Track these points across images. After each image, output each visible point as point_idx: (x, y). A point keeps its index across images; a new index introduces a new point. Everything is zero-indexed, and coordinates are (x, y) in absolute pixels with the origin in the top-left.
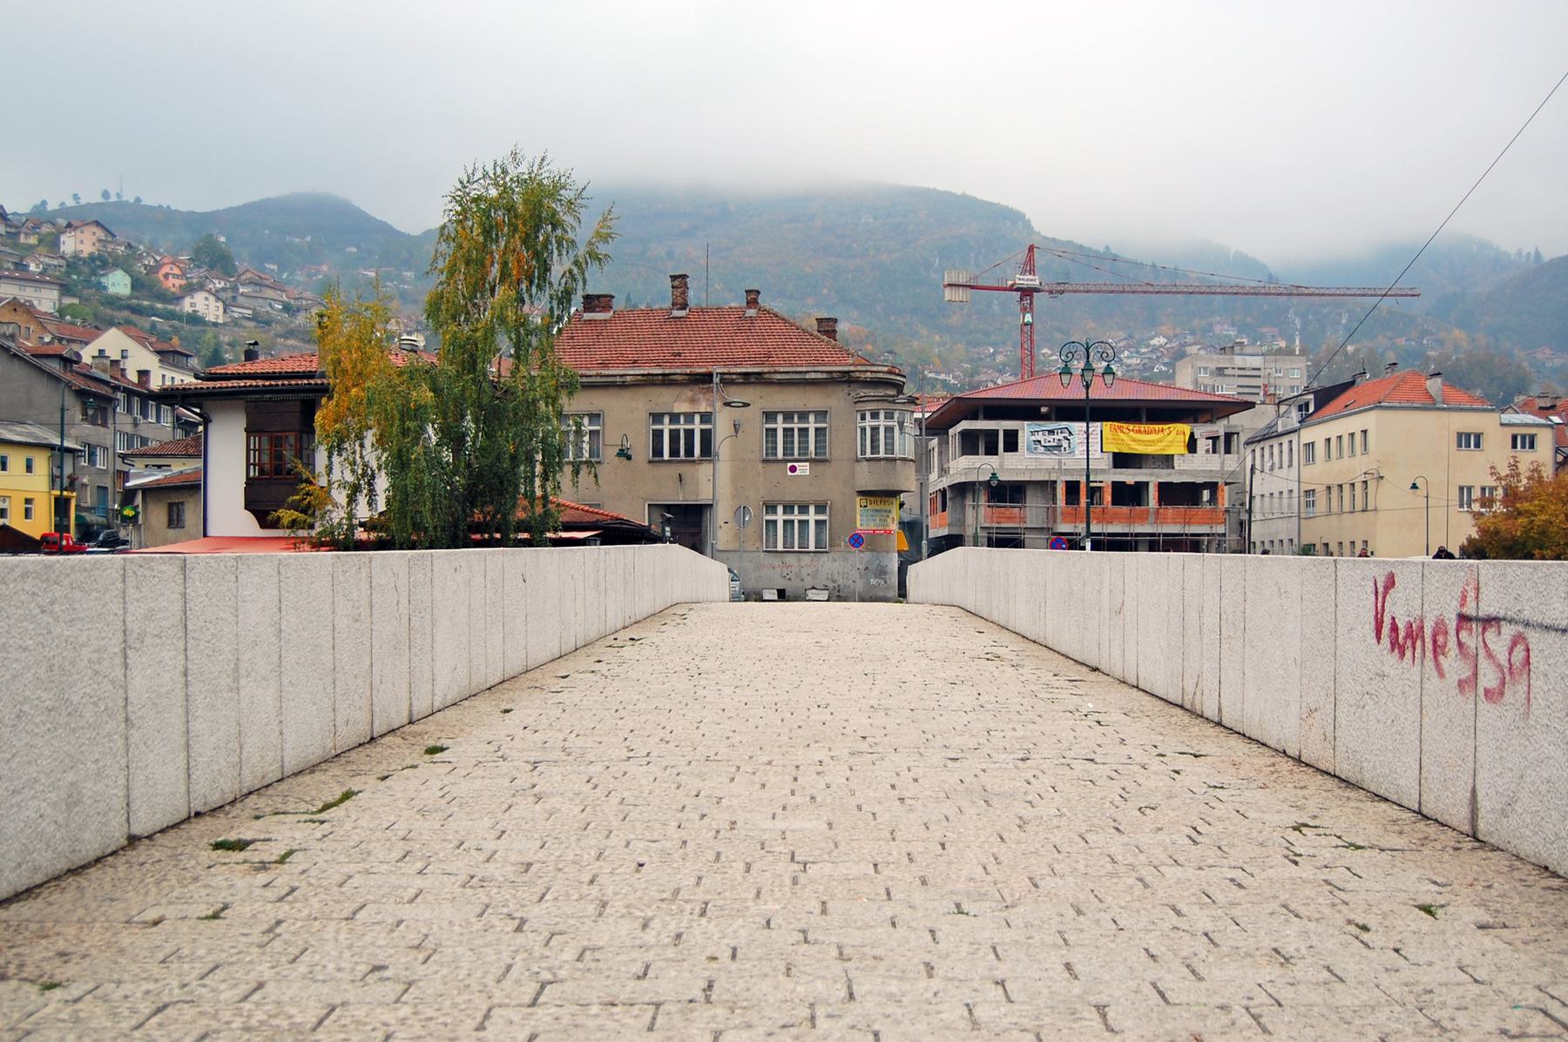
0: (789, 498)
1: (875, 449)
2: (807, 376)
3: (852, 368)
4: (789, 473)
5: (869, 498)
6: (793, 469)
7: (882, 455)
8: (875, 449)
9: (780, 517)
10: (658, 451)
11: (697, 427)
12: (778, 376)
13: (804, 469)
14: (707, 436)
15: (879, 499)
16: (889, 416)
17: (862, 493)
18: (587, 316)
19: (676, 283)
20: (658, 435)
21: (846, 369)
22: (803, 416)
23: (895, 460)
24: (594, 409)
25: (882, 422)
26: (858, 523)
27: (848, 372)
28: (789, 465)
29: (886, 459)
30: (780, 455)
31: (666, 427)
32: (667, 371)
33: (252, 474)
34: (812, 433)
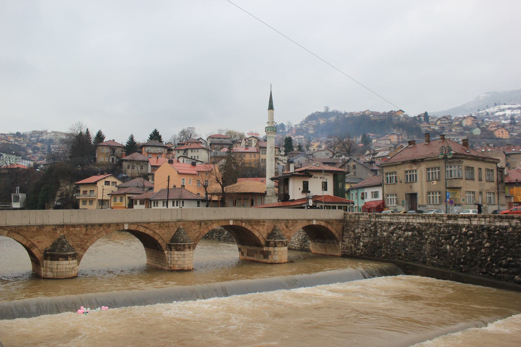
0: (433, 190)
6: (433, 183)
7: (449, 178)
12: (429, 159)
14: (416, 175)
19: (426, 136)
20: (407, 176)
22: (435, 168)
24: (395, 171)
28: (432, 182)
29: (450, 179)
30: (431, 179)
34: (437, 173)
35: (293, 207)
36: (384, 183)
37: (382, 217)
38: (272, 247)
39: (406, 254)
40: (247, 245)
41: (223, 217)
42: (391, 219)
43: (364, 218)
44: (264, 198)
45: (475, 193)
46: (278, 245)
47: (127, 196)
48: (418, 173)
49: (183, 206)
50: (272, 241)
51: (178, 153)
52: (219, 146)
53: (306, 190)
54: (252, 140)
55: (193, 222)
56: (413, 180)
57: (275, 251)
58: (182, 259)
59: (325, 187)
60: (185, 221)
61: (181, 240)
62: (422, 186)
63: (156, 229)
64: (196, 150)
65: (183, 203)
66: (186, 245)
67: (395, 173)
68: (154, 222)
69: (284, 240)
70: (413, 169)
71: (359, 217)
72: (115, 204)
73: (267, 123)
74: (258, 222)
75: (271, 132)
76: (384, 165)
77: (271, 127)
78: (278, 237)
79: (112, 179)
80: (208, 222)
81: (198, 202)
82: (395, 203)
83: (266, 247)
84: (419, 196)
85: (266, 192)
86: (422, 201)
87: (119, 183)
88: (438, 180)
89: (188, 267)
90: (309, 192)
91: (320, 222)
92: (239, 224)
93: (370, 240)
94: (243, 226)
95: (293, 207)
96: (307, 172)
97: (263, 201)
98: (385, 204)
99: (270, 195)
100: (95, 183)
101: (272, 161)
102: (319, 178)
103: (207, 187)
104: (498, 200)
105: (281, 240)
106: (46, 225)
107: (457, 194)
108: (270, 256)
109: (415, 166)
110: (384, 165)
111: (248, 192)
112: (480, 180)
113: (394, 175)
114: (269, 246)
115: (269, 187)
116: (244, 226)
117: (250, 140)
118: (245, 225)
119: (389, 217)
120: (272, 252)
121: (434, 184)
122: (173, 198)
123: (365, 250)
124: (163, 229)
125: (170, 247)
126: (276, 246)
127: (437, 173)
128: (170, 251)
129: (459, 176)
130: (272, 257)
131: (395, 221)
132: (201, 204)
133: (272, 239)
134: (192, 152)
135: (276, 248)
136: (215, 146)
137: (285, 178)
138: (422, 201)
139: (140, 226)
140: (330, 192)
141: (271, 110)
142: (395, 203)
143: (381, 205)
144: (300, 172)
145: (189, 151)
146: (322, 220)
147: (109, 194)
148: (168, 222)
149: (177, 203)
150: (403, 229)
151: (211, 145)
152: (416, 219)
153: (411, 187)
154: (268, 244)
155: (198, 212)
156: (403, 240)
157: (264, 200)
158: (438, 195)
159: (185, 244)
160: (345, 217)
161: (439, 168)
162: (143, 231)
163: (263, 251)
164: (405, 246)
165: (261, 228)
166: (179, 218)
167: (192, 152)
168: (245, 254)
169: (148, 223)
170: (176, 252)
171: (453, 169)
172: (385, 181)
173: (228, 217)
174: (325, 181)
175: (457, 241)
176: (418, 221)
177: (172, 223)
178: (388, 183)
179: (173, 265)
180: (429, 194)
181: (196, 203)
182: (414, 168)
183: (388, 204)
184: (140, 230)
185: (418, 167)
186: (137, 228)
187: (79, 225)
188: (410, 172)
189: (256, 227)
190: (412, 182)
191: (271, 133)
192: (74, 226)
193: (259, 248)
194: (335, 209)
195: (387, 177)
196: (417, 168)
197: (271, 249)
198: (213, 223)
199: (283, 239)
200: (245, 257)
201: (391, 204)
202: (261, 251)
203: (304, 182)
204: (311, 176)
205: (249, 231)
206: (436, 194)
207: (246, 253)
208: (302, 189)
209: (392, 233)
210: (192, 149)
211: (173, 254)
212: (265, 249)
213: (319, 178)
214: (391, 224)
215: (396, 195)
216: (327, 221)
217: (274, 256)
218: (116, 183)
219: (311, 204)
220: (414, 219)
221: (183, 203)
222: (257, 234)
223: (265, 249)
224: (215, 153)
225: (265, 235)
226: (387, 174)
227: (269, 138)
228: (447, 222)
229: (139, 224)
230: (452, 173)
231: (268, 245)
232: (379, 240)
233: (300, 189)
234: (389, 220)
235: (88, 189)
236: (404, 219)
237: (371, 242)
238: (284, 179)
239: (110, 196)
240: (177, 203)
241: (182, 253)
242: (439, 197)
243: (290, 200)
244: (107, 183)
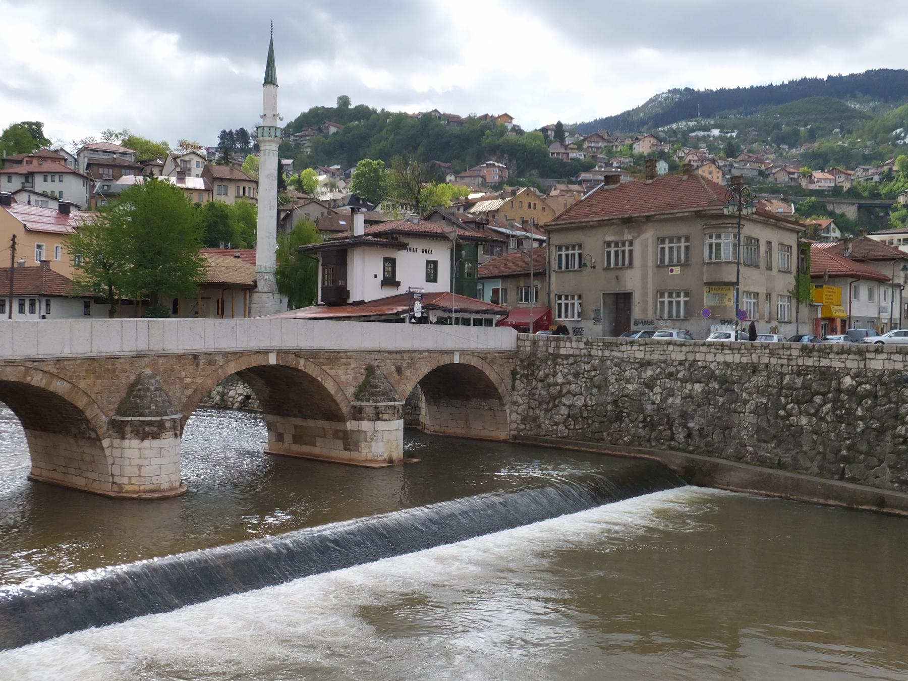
1: (710, 258)
2: (677, 215)
3: (701, 209)
4: (670, 273)
5: (711, 287)
6: (672, 271)
7: (714, 260)
8: (710, 258)
9: (666, 299)
10: (609, 264)
11: (627, 248)
13: (677, 270)
14: (631, 252)
15: (717, 287)
16: (719, 237)
17: (707, 284)
18: (606, 187)
19: (648, 164)
20: (609, 253)
21: (698, 209)
23: (721, 263)
25: (714, 241)
26: (705, 302)
27: (699, 211)
31: (613, 249)
32: (611, 217)
33: (326, 284)
35: (372, 318)
36: (552, 269)
37: (623, 348)
38: (370, 420)
39: (689, 436)
40: (295, 416)
41: (254, 343)
42: (645, 351)
43: (572, 348)
44: (250, 296)
45: (759, 296)
46: (385, 417)
48: (637, 247)
49: (48, 312)
50: (368, 406)
51: (9, 181)
52: (111, 171)
54: (190, 161)
55: (180, 357)
56: (623, 263)
57: (375, 431)
58: (155, 461)
60: (157, 356)
61: (150, 407)
62: (644, 276)
63: (78, 377)
65: (48, 305)
66: (166, 420)
67: (580, 247)
68: (75, 359)
69: (397, 403)
70: (625, 239)
71: (558, 347)
73: (261, 117)
74: (333, 358)
75: (270, 138)
76: (553, 227)
77: (270, 128)
78: (383, 395)
80: (217, 357)
81: (85, 302)
82: (576, 315)
83: (353, 422)
84: (636, 299)
85: (255, 282)
86: (645, 310)
88: (685, 265)
89: (171, 482)
90: (398, 284)
91: (468, 357)
92: (291, 361)
93: (590, 403)
94: (300, 368)
95: (372, 318)
96: (394, 235)
97: (249, 304)
98: (553, 317)
99: (266, 289)
101: (270, 209)
102: (420, 250)
103: (110, 266)
104: (797, 312)
105: (392, 403)
107: (727, 297)
108: (363, 445)
109: (630, 233)
110: (553, 227)
111: (216, 280)
112: (769, 268)
113: (577, 252)
114: (361, 419)
115: (263, 270)
116: (303, 368)
117: (185, 161)
118: (305, 366)
119: (642, 348)
120: (369, 434)
121: (674, 273)
122: (21, 292)
123: (574, 425)
124: (98, 378)
125: (119, 429)
126: (378, 419)
127: (667, 251)
128: (118, 441)
130: (370, 447)
131: (656, 357)
132: (93, 307)
133: (368, 400)
134: (45, 180)
135: (379, 422)
136: (101, 171)
137: (339, 248)
138: (645, 310)
139: (33, 371)
140: (443, 284)
141: (272, 86)
142: (576, 315)
143: (545, 318)
144: (376, 235)
145: (38, 180)
146: (472, 353)
148: (112, 359)
149: (32, 304)
150: (680, 375)
151: (89, 166)
152: (715, 354)
153: (617, 278)
154: (358, 414)
155: (191, 329)
156: (678, 401)
157: (250, 301)
158: (682, 299)
159: (164, 418)
160: (518, 347)
161: (687, 239)
162: (42, 385)
163: (345, 432)
164: (685, 416)
165: (341, 373)
166: (143, 346)
167: (45, 180)
168: (288, 438)
169: (58, 361)
170: (136, 443)
171: (723, 240)
172: (554, 265)
173: (263, 344)
174: (432, 257)
175: (829, 406)
176: (720, 358)
177: (122, 361)
178: (560, 267)
179: (130, 478)
180: (662, 295)
181: (80, 308)
182: (628, 237)
183: (560, 316)
184: (32, 383)
185: (636, 234)
186: (25, 377)
188: (617, 245)
189: (331, 369)
190: (621, 268)
193: (333, 423)
194: (469, 324)
195: (560, 256)
196: (635, 238)
197: (366, 426)
198: (227, 361)
199: (395, 400)
200: (286, 445)
201: (566, 317)
202: (337, 431)
203: (386, 260)
204: (403, 246)
205: (313, 380)
206: (678, 295)
207: (291, 437)
208: (381, 277)
209: (649, 384)
210: (45, 175)
211: (130, 448)
212: (351, 425)
213: (420, 250)
214: (645, 364)
215: (580, 297)
216: (483, 355)
217: (373, 444)
219: (418, 314)
220: (710, 352)
221: (48, 305)
222: (330, 386)
223: (351, 425)
224: (106, 188)
225: (351, 391)
226: (560, 249)
227: (265, 154)
228: (800, 362)
229: (29, 364)
230: (720, 249)
231: (360, 416)
232: (615, 402)
233: (376, 276)
234: (639, 355)
236: (681, 352)
237: (592, 406)
238: (338, 251)
240: (32, 304)
241: (156, 443)
242: (685, 302)
243: (351, 301)
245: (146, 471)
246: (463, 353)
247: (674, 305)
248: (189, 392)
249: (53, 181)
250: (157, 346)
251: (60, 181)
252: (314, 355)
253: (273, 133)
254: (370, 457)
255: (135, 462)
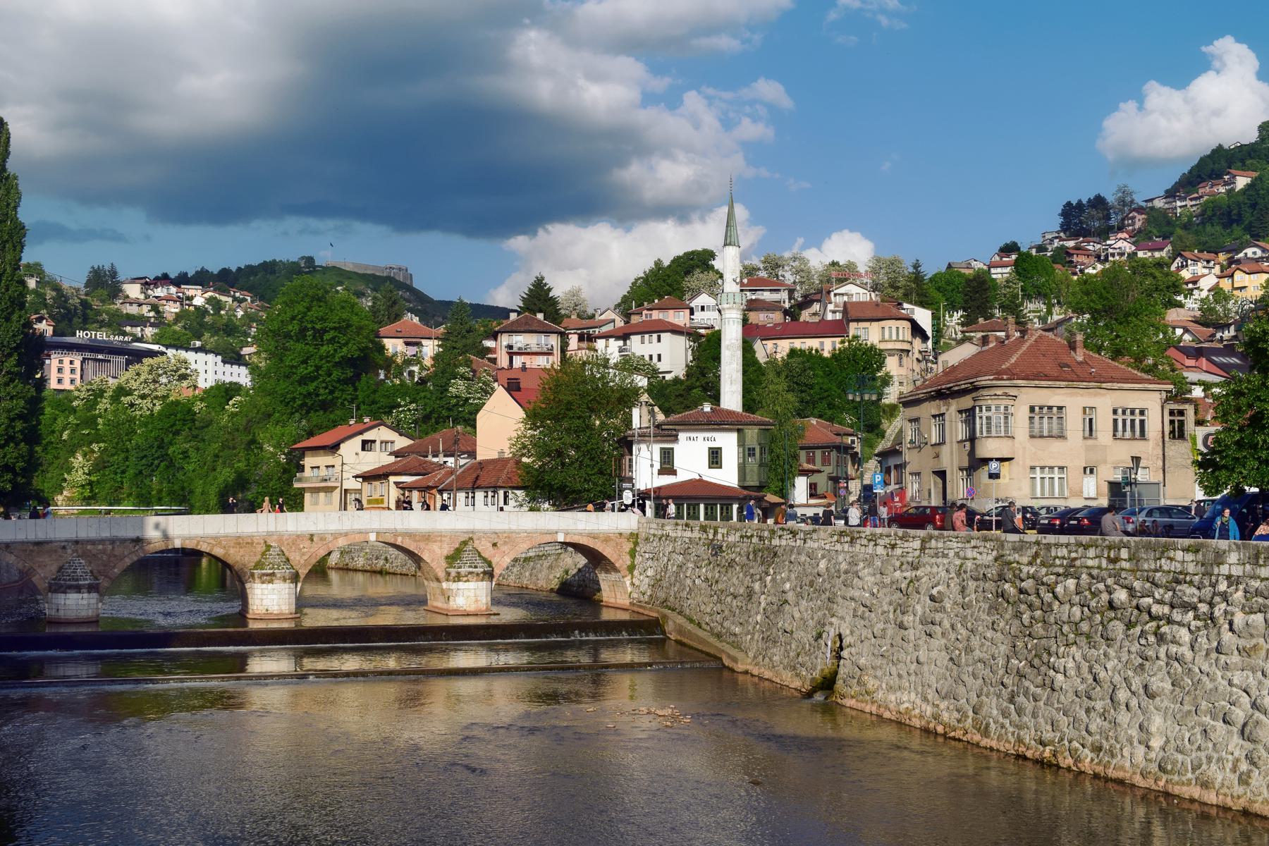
41: (357, 526)
47: (392, 479)
53: (667, 465)
59: (715, 458)
64: (655, 336)
72: (369, 502)
79: (381, 434)
87: (402, 442)
100: (334, 448)
106: (51, 542)
126: (459, 581)
129: (1006, 431)
147: (356, 477)
148: (252, 537)
169: (215, 538)
187: (102, 541)
191: (729, 308)
192: (93, 542)
197: (454, 586)
208: (657, 466)
218: (392, 442)
221: (506, 497)
223: (445, 585)
235: (322, 460)
239: (361, 480)
241: (270, 586)
244: (366, 445)
245: (265, 602)
246: (566, 534)
247: (1047, 481)
248: (306, 557)
249: (650, 342)
250: (281, 528)
251: (659, 340)
252: (410, 535)
253: (731, 300)
254: (455, 607)
255: (260, 597)
